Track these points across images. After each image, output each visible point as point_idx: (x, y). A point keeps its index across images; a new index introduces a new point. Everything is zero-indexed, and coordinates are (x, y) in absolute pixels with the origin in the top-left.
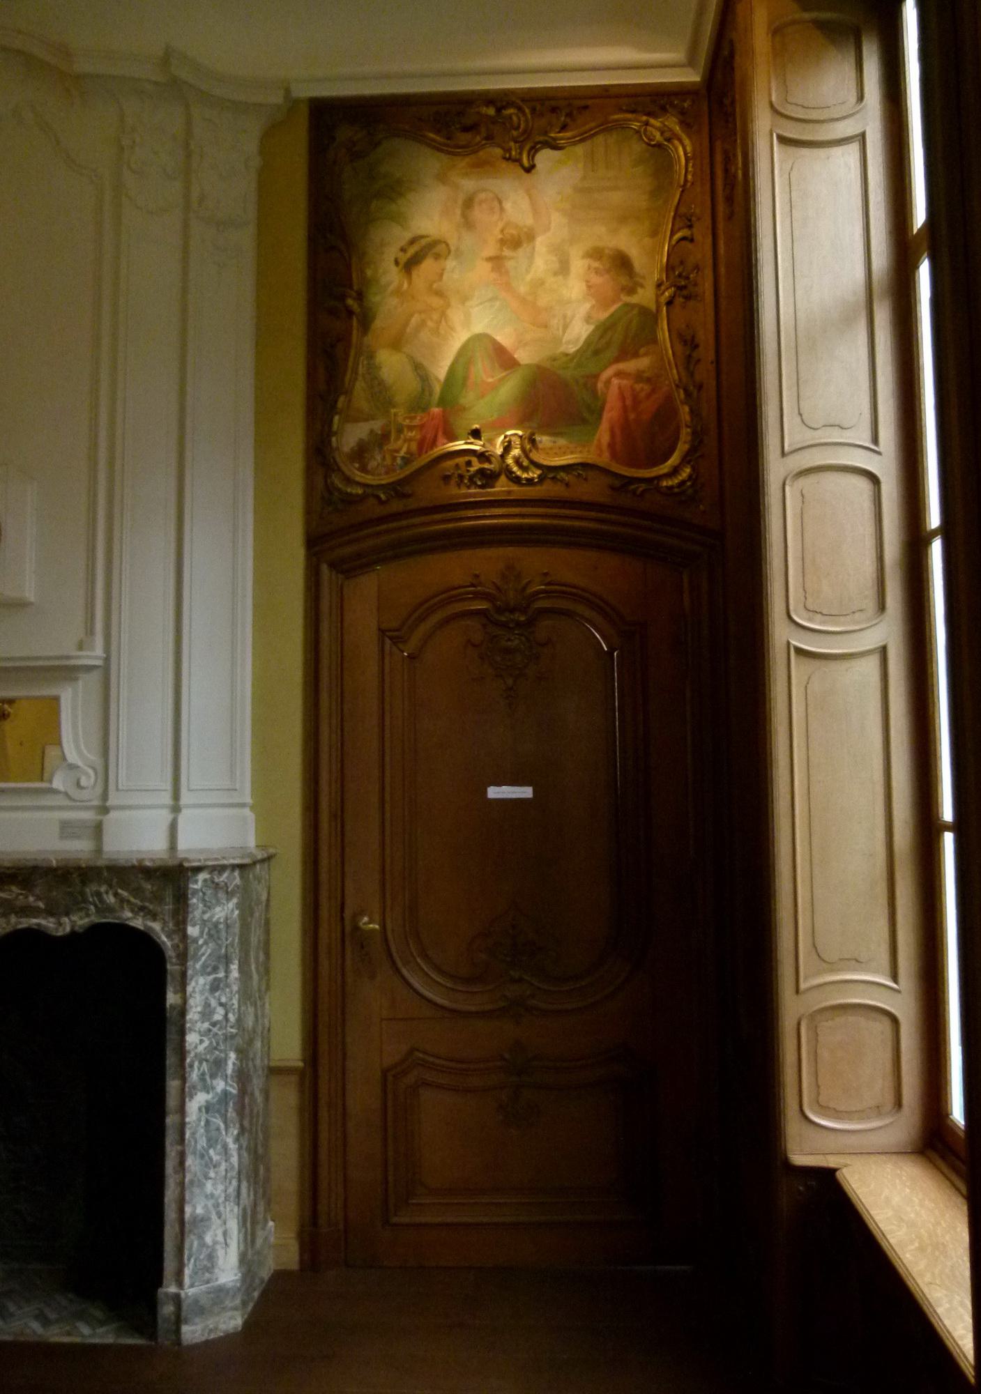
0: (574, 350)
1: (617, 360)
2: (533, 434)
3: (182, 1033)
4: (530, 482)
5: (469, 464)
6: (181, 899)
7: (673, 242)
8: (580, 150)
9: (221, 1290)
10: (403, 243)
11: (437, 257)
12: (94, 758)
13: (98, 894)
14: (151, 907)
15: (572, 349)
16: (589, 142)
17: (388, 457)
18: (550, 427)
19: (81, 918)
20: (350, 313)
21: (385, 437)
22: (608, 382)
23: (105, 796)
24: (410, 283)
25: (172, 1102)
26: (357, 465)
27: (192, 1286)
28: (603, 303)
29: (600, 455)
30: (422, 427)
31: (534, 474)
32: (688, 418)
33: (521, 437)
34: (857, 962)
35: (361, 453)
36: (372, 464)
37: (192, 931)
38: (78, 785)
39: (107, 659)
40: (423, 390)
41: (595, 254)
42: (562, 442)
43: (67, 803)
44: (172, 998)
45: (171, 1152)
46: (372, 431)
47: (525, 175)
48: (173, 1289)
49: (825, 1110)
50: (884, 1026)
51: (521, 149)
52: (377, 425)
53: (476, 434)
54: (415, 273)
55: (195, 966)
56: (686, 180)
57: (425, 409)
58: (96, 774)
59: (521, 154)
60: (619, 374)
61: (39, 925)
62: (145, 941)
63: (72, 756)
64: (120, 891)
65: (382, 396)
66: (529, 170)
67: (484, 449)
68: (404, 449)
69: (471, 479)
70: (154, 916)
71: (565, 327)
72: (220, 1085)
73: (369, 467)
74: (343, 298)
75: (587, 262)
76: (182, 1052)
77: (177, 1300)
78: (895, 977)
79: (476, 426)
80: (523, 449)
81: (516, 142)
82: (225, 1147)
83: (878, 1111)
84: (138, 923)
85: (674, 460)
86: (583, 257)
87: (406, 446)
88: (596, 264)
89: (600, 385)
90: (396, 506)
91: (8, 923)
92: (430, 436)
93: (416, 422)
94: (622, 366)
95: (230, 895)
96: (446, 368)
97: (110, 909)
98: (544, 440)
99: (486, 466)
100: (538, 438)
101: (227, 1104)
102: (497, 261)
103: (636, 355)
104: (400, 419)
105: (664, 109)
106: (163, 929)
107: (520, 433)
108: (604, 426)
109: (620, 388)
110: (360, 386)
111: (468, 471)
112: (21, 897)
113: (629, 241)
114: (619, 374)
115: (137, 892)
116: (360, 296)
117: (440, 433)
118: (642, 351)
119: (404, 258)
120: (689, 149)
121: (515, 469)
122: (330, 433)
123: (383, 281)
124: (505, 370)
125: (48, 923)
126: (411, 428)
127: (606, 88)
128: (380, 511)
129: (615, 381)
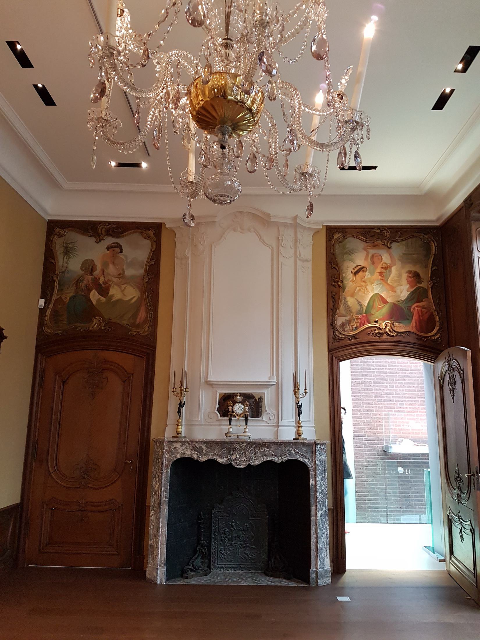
0: (404, 299)
1: (417, 302)
2: (394, 323)
3: (316, 492)
4: (393, 336)
5: (375, 330)
6: (314, 452)
7: (432, 270)
8: (404, 243)
9: (326, 570)
10: (354, 267)
11: (363, 271)
12: (275, 412)
13: (289, 450)
14: (305, 455)
15: (403, 299)
16: (406, 241)
17: (351, 327)
18: (398, 320)
19: (285, 458)
20: (339, 286)
21: (350, 322)
23: (278, 422)
24: (356, 278)
25: (313, 513)
26: (342, 329)
27: (320, 569)
28: (412, 287)
29: (413, 329)
30: (360, 319)
31: (395, 334)
32: (438, 320)
33: (390, 323)
35: (343, 325)
36: (346, 329)
37: (317, 462)
39: (277, 383)
40: (360, 309)
41: (410, 272)
42: (401, 325)
44: (312, 482)
45: (313, 528)
47: (389, 249)
48: (314, 569)
51: (388, 242)
52: (347, 318)
53: (377, 322)
54: (357, 276)
55: (318, 472)
56: (435, 253)
57: (361, 314)
58: (274, 416)
59: (388, 244)
60: (417, 306)
61: (273, 459)
62: (303, 464)
64: (296, 450)
65: (349, 311)
66: (390, 248)
67: (379, 326)
68: (356, 325)
69: (376, 334)
70: (306, 458)
72: (324, 509)
73: (345, 330)
74: (337, 282)
75: (407, 274)
76: (316, 498)
77: (317, 573)
79: (376, 320)
80: (391, 327)
81: (386, 240)
82: (326, 527)
84: (301, 459)
85: (435, 331)
86: (406, 273)
87: (356, 324)
88: (410, 275)
89: (412, 309)
90: (354, 341)
91: (264, 459)
92: (363, 322)
93: (359, 318)
94: (418, 304)
95: (325, 452)
96: (367, 303)
97: (293, 455)
98: (396, 324)
99: (380, 331)
100: (395, 323)
101: (326, 515)
102: (381, 273)
103: (422, 301)
104: (354, 317)
105: (428, 233)
106: (308, 461)
107: (390, 322)
108: (414, 321)
109: (417, 310)
110: (342, 307)
111: (375, 332)
112: (267, 451)
113: (417, 269)
114: (417, 306)
115: (301, 450)
116: (342, 282)
117: (366, 321)
118: (423, 300)
119: (354, 271)
120: (436, 244)
121: (389, 332)
122: (335, 320)
123: (348, 278)
124: (384, 304)
125: (275, 459)
127: (412, 226)
128: (349, 342)
129: (416, 308)
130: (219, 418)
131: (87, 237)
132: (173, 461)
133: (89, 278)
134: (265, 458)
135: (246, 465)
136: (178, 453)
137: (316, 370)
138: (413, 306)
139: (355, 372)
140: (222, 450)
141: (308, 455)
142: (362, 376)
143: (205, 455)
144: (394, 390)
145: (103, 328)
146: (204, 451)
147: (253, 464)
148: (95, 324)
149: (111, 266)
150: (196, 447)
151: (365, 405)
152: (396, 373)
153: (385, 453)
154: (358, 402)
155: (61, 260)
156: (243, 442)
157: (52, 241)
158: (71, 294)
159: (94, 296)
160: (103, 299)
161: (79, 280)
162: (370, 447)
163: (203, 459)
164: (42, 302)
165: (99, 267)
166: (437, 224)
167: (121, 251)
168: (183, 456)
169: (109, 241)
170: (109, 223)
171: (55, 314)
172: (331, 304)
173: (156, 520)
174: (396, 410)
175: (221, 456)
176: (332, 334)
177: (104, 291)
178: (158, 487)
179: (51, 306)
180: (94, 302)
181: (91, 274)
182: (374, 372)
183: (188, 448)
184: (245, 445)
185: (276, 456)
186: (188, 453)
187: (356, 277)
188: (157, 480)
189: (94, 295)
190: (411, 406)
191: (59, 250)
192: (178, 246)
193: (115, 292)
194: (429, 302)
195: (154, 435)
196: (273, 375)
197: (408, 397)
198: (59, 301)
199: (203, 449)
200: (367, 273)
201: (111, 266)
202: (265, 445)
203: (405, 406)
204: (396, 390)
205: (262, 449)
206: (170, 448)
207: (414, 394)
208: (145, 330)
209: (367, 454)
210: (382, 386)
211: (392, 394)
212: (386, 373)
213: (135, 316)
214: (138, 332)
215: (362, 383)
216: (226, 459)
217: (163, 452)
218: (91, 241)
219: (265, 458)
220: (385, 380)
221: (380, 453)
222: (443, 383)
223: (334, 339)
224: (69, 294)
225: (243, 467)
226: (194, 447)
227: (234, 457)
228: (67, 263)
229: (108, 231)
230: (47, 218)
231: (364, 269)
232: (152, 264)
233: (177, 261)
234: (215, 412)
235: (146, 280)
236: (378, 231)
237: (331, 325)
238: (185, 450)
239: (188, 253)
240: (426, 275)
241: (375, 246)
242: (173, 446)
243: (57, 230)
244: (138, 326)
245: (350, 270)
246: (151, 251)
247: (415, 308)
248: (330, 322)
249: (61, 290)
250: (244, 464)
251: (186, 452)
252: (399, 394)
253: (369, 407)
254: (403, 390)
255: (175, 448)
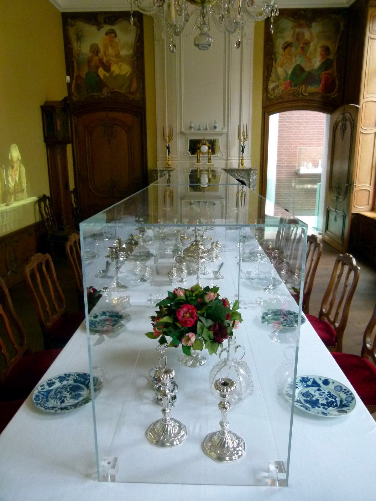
1: (324, 71)
6: (249, 175)
12: (226, 151)
13: (234, 174)
22: (323, 75)
23: (227, 157)
28: (323, 59)
31: (307, 94)
34: (365, 183)
35: (273, 89)
37: (251, 180)
38: (222, 155)
39: (228, 132)
43: (219, 159)
46: (276, 85)
49: (358, 205)
50: (368, 192)
52: (277, 84)
60: (325, 74)
63: (221, 150)
70: (244, 178)
71: (315, 63)
74: (271, 56)
78: (370, 185)
83: (365, 205)
85: (334, 92)
90: (280, 100)
94: (326, 72)
95: (256, 174)
104: (281, 83)
119: (283, 47)
122: (268, 85)
126: (283, 84)
129: (324, 75)
130: (190, 155)
131: (91, 26)
133: (96, 59)
137: (254, 122)
138: (322, 74)
139: (282, 120)
141: (246, 176)
142: (287, 122)
144: (307, 132)
145: (110, 96)
148: (105, 92)
149: (110, 48)
151: (286, 143)
152: (310, 119)
153: (297, 175)
154: (282, 141)
155: (75, 45)
157: (67, 30)
158: (86, 72)
159: (101, 72)
160: (107, 74)
161: (89, 61)
162: (288, 171)
164: (68, 78)
165: (102, 50)
166: (347, 6)
167: (116, 36)
169: (107, 28)
170: (106, 13)
171: (78, 87)
172: (266, 74)
174: (307, 145)
176: (266, 95)
177: (107, 68)
179: (74, 81)
180: (102, 77)
181: (97, 55)
182: (295, 119)
187: (285, 51)
189: (101, 71)
190: (317, 143)
191: (73, 37)
192: (156, 30)
193: (115, 68)
194: (334, 70)
195: (150, 166)
196: (225, 126)
197: (316, 137)
198: (79, 77)
200: (293, 48)
201: (110, 48)
203: (313, 143)
204: (309, 132)
206: (161, 174)
207: (320, 134)
208: (138, 96)
209: (285, 175)
210: (299, 129)
211: (306, 134)
212: (303, 119)
213: (130, 86)
214: (133, 98)
215: (286, 127)
217: (157, 177)
218: (94, 28)
220: (302, 124)
221: (293, 174)
222: (336, 128)
223: (267, 99)
224: (84, 71)
228: (80, 47)
229: (105, 19)
230: (61, 11)
231: (291, 45)
232: (138, 46)
233: (156, 42)
234: (187, 152)
235: (135, 58)
236: (304, 13)
237: (265, 89)
239: (164, 36)
240: (333, 49)
241: (300, 26)
243: (69, 21)
244: (132, 94)
245: (281, 45)
246: (137, 35)
247: (323, 74)
248: (265, 86)
249: (79, 68)
252: (310, 134)
253: (289, 144)
254: (313, 132)
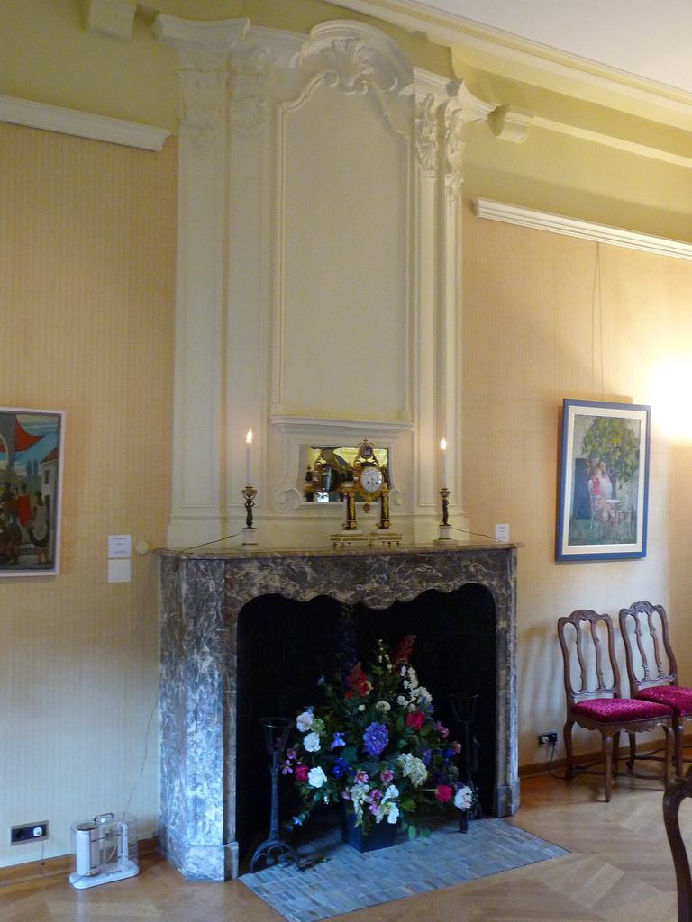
132: (243, 604)
134: (425, 585)
135: (390, 602)
136: (253, 585)
140: (344, 573)
143: (311, 586)
146: (309, 578)
147: (403, 599)
150: (293, 570)
156: (385, 555)
163: (310, 595)
168: (264, 591)
173: (207, 742)
175: (342, 588)
178: (210, 666)
183: (274, 572)
184: (387, 559)
185: (443, 579)
186: (276, 584)
188: (206, 649)
199: (307, 573)
202: (424, 558)
205: (420, 567)
216: (353, 593)
219: (425, 585)
225: (386, 607)
226: (287, 571)
227: (367, 587)
238: (268, 578)
242: (242, 569)
250: (387, 600)
251: (271, 582)
255: (246, 575)
